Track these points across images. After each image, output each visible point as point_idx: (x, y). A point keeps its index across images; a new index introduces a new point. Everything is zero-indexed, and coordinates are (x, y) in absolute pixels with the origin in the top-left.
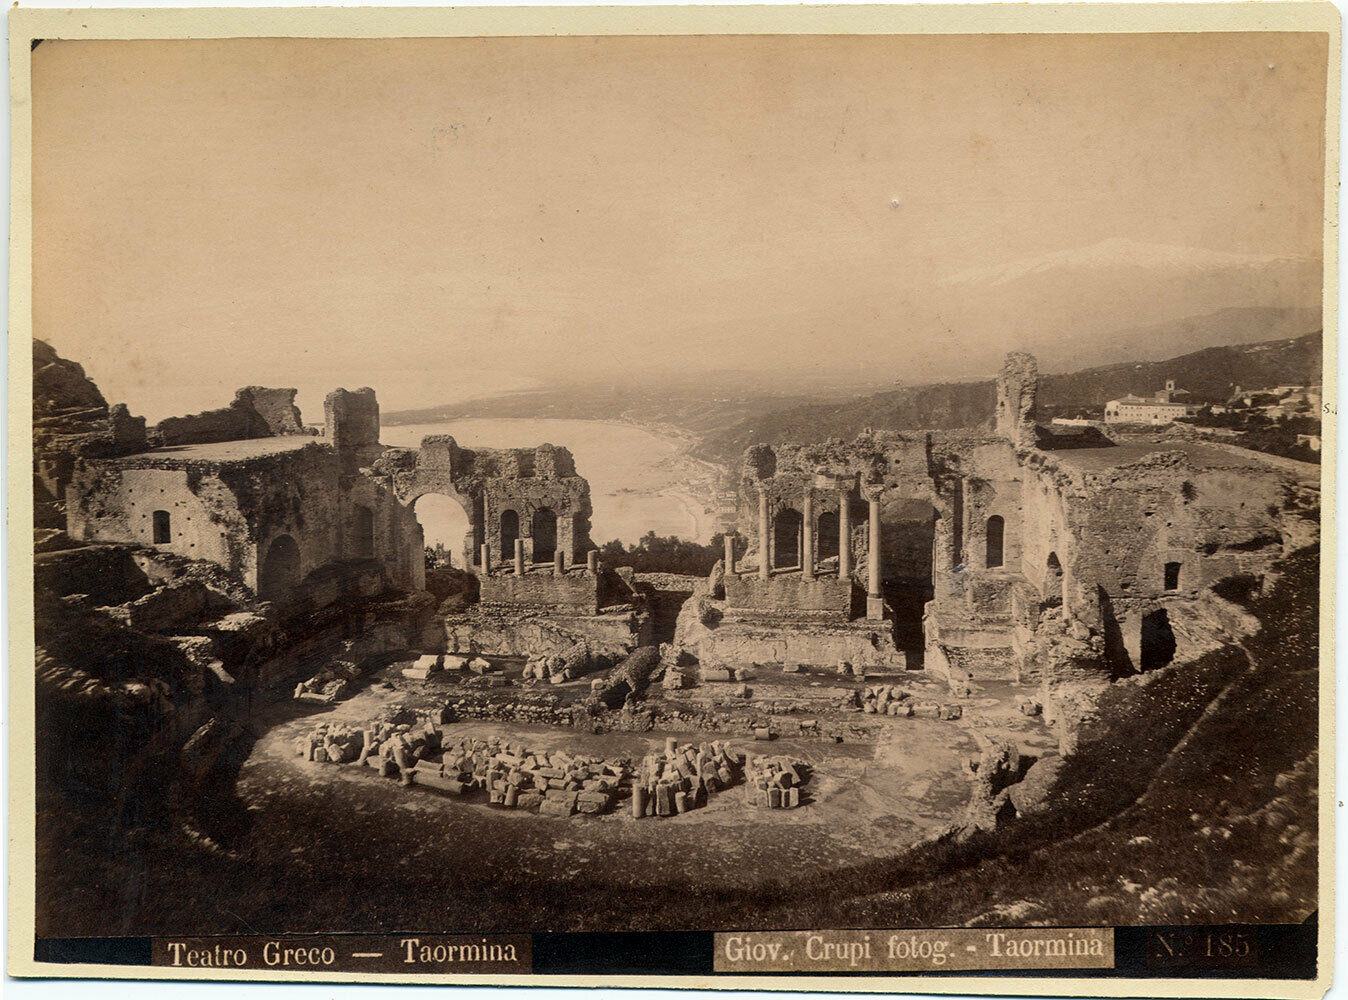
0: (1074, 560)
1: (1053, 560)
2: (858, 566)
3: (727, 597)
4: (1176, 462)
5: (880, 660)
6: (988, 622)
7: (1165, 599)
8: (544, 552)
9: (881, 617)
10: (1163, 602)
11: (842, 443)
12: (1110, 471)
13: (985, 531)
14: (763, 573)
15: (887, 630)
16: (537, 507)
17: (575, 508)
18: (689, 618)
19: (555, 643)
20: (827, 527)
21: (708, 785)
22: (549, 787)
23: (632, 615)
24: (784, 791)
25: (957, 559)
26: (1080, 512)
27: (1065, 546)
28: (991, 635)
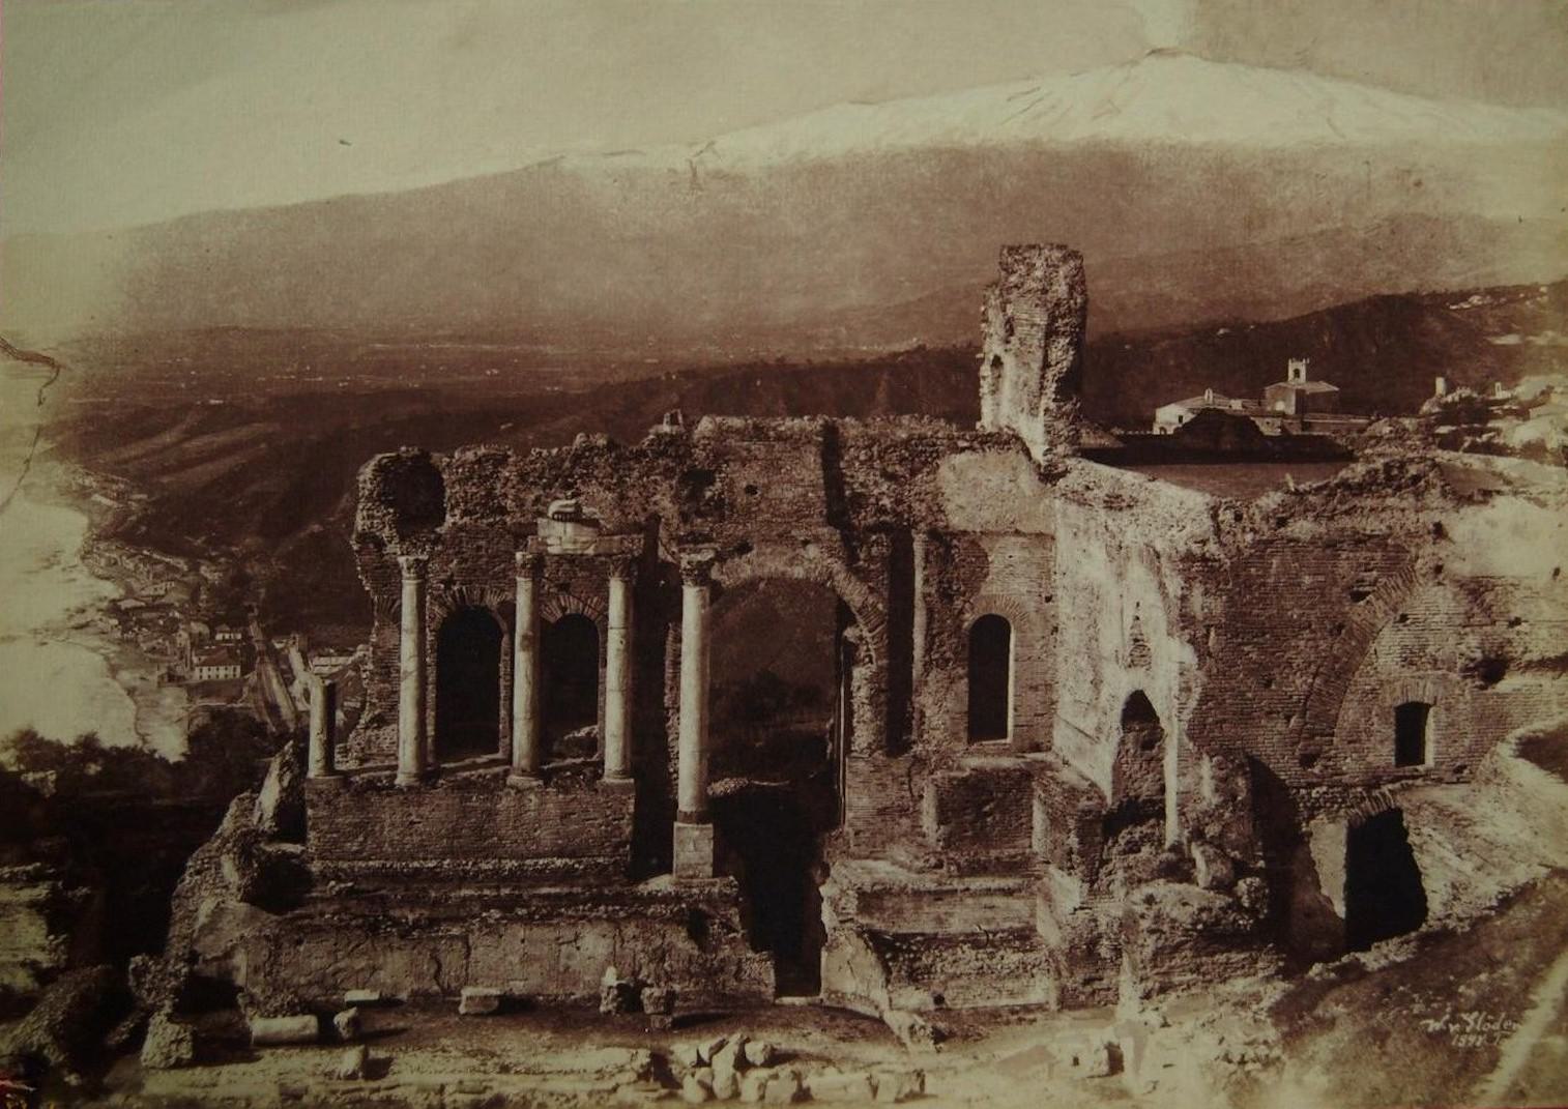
1: (1138, 710)
12: (1271, 500)
23: (53, 889)
27: (1171, 673)
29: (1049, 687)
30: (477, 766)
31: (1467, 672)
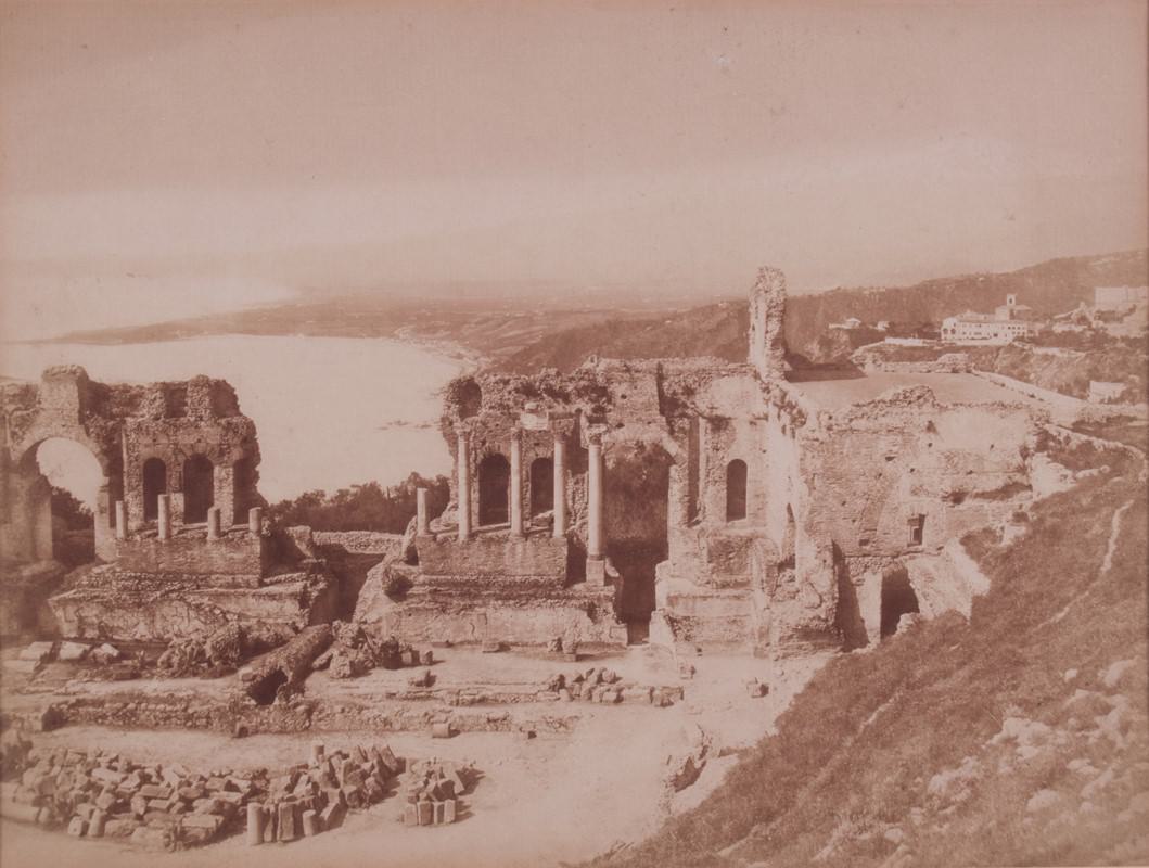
0: (806, 513)
2: (579, 523)
3: (420, 563)
4: (919, 397)
5: (599, 634)
6: (724, 586)
7: (907, 557)
8: (197, 508)
9: (602, 583)
10: (906, 560)
11: (558, 374)
13: (725, 478)
14: (463, 532)
15: (608, 599)
16: (189, 453)
17: (236, 454)
18: (372, 590)
19: (205, 623)
20: (540, 473)
21: (349, 799)
22: (148, 810)
23: (305, 587)
24: (436, 804)
25: (692, 513)
26: (813, 457)
28: (728, 601)
29: (764, 495)
30: (492, 532)
31: (944, 499)
